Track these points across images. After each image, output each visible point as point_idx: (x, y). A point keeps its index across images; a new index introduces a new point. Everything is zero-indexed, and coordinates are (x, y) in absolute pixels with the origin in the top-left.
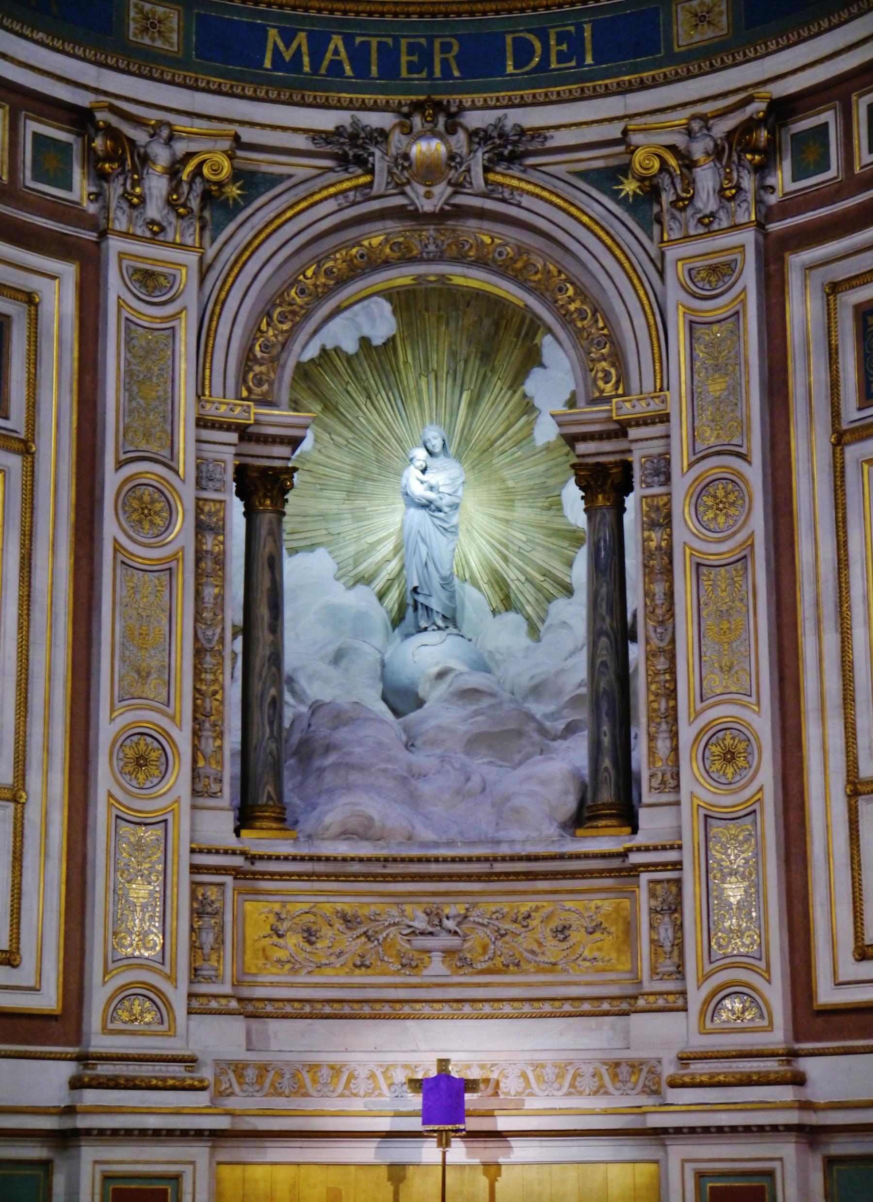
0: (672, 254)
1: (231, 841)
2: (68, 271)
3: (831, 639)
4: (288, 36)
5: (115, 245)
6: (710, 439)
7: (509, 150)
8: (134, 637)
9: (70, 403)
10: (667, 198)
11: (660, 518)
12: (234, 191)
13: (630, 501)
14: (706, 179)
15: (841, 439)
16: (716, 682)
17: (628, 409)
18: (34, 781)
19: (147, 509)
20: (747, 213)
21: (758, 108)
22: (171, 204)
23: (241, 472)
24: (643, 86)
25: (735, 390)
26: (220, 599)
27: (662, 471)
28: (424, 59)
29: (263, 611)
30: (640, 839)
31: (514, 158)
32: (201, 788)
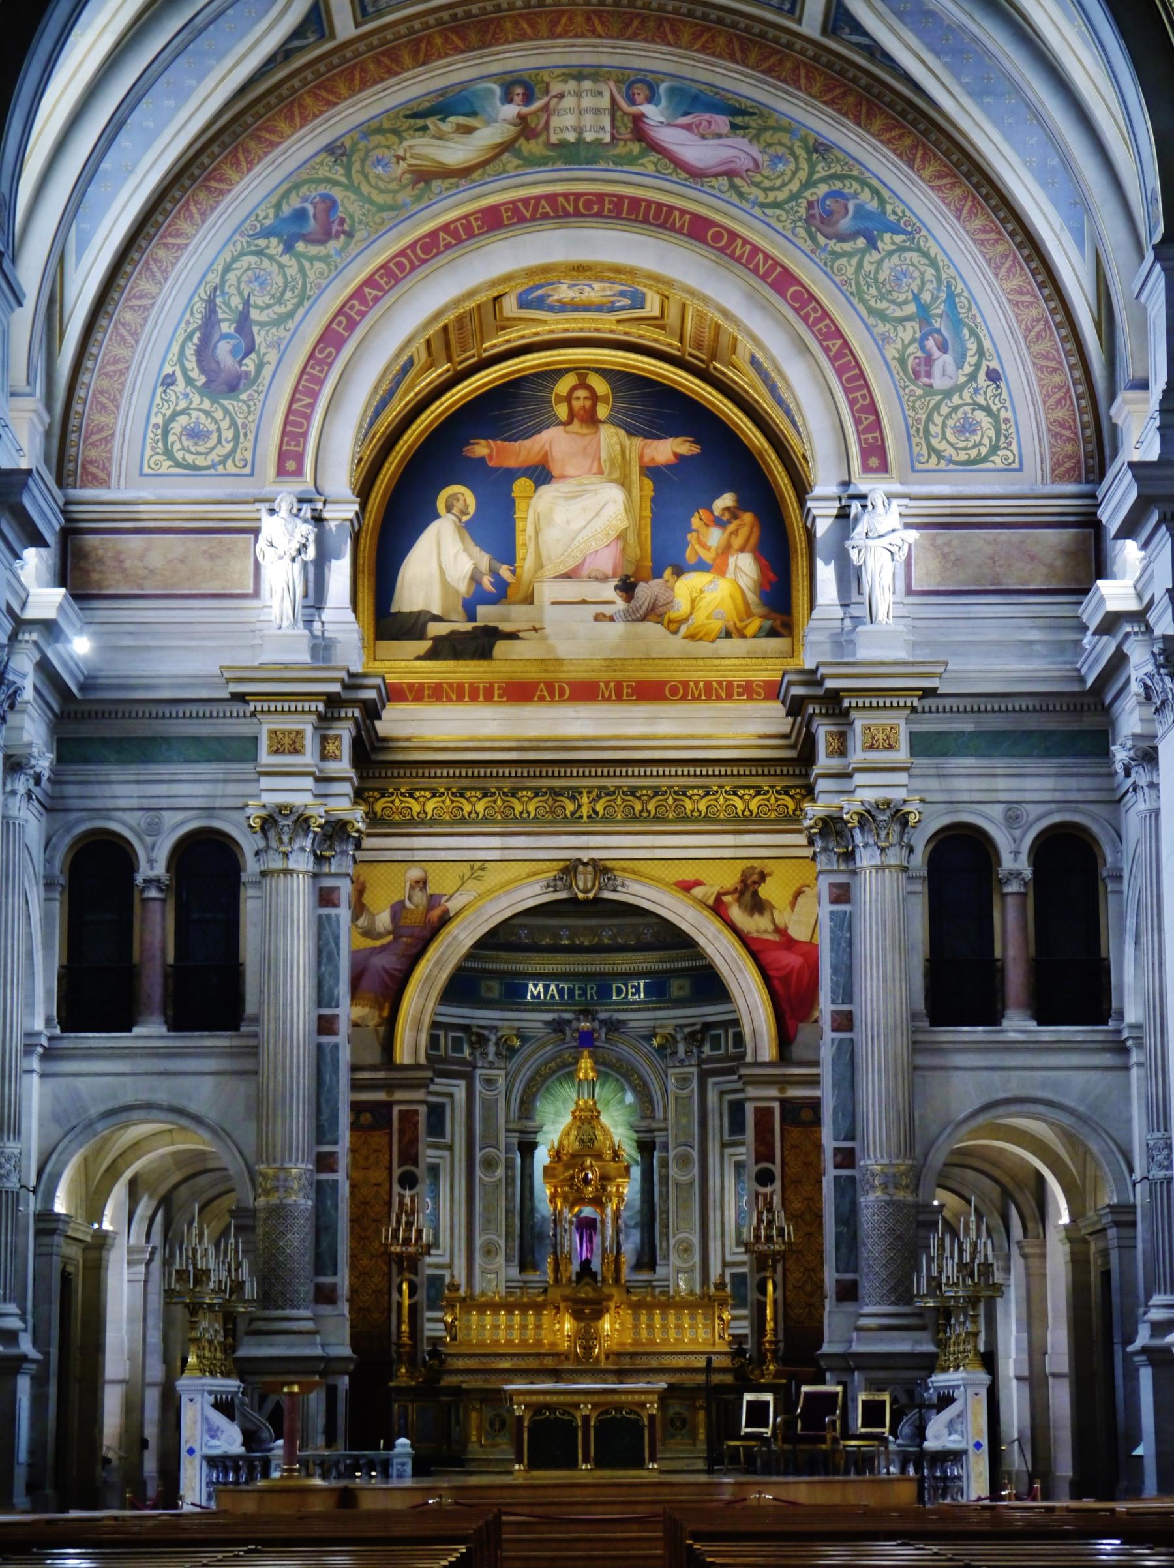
0: (670, 1071)
1: (518, 1277)
2: (462, 1083)
3: (718, 1214)
4: (536, 986)
5: (478, 1072)
6: (682, 1140)
7: (614, 1026)
8: (486, 1209)
9: (463, 1129)
10: (669, 1051)
11: (664, 1164)
12: (517, 1043)
13: (656, 1154)
14: (681, 1048)
15: (724, 1145)
16: (682, 1225)
17: (655, 1125)
18: (456, 1261)
19: (489, 1164)
20: (694, 1061)
21: (698, 1027)
22: (497, 1054)
23: (520, 1144)
24: (660, 1009)
25: (690, 1123)
26: (514, 1194)
27: (665, 1147)
28: (584, 993)
29: (527, 1194)
30: (657, 1277)
31: (617, 1030)
32: (508, 1259)
